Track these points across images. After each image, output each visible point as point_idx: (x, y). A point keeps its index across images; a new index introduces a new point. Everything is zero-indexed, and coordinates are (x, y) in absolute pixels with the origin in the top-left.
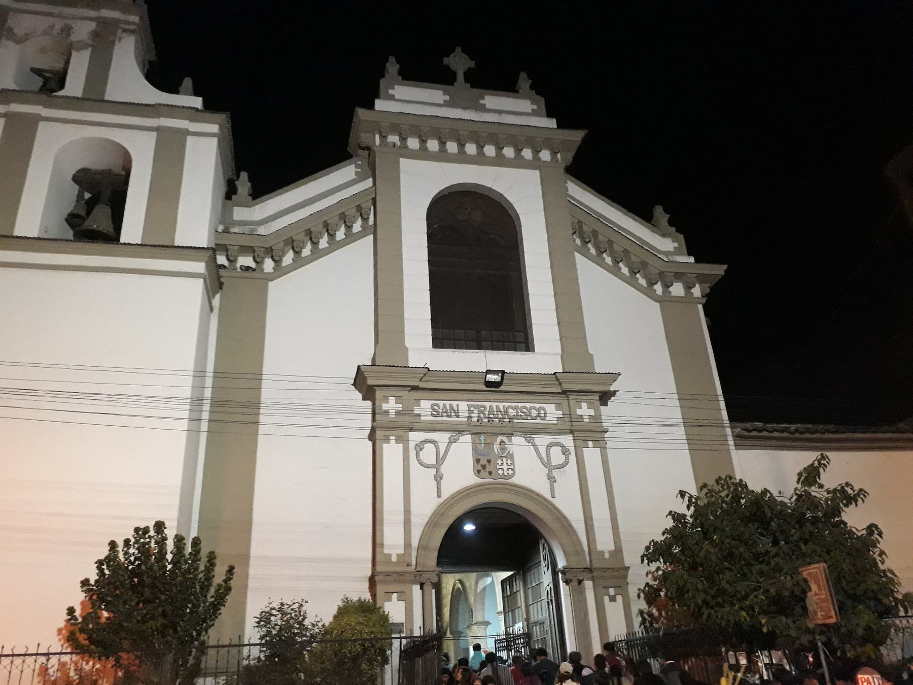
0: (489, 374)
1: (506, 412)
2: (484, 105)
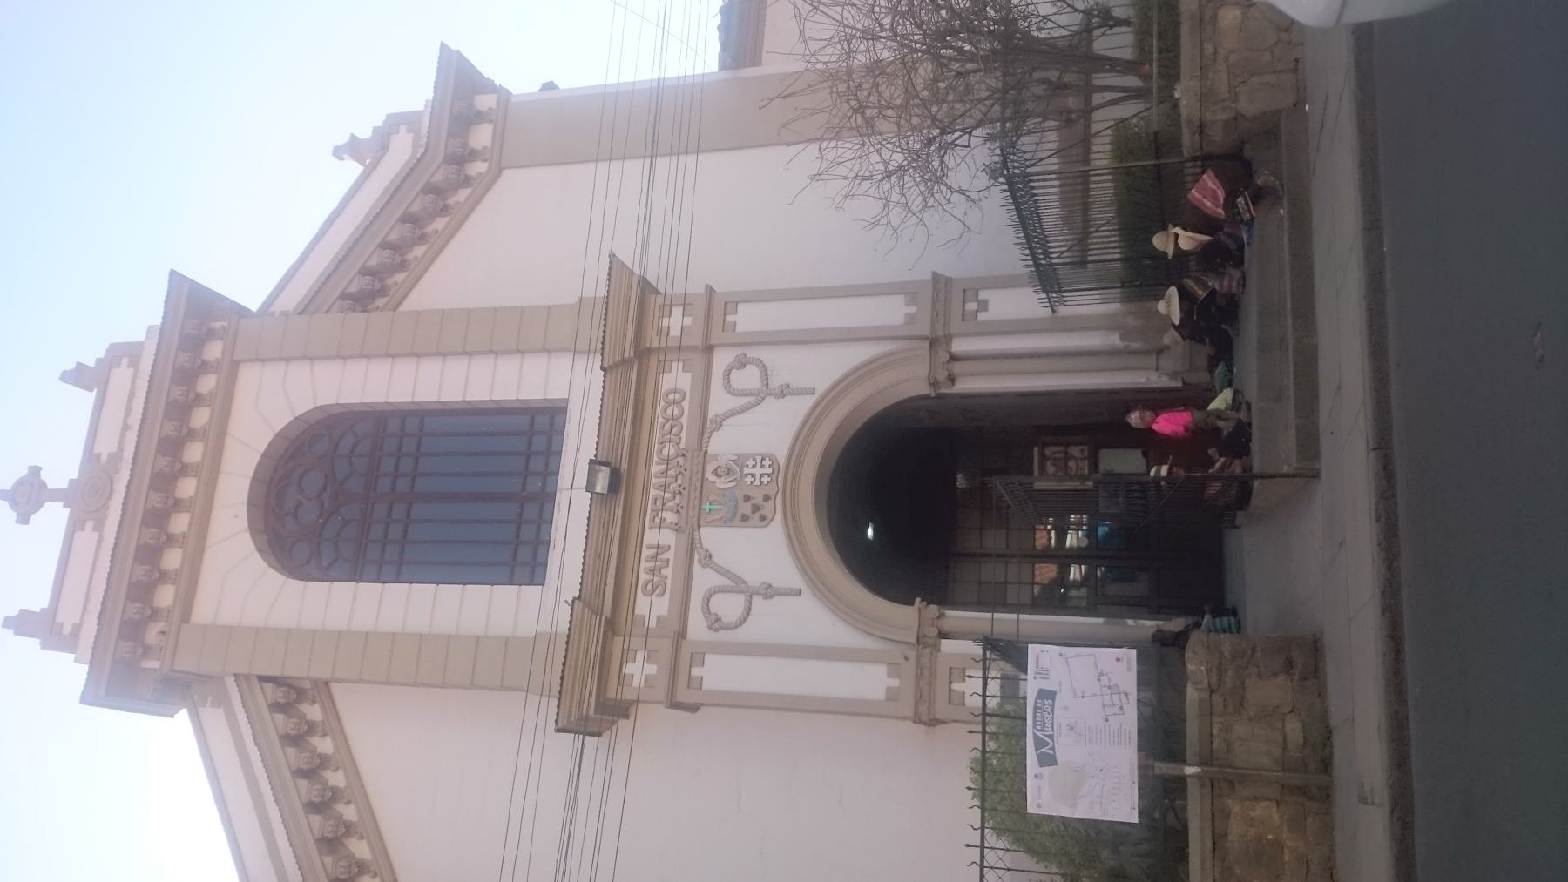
0: (594, 486)
1: (668, 461)
2: (110, 455)
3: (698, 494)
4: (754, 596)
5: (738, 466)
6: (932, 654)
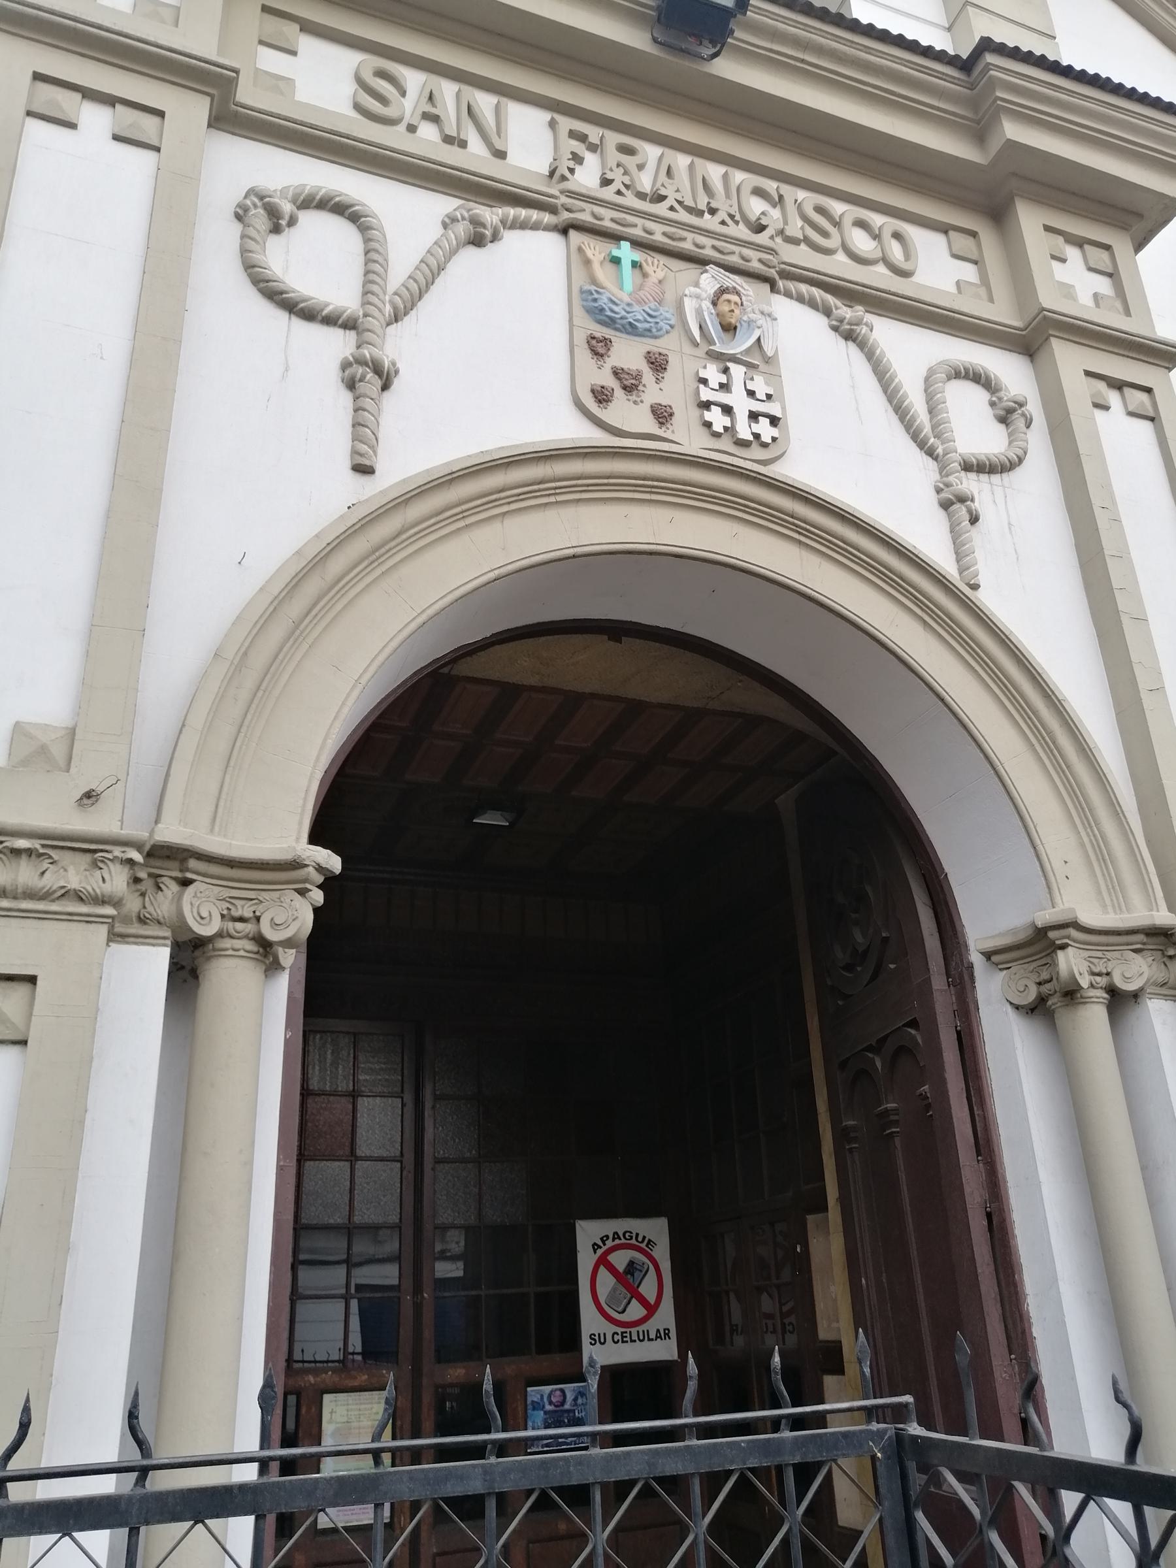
3: (658, 238)
4: (351, 335)
5: (748, 351)
6: (102, 901)
